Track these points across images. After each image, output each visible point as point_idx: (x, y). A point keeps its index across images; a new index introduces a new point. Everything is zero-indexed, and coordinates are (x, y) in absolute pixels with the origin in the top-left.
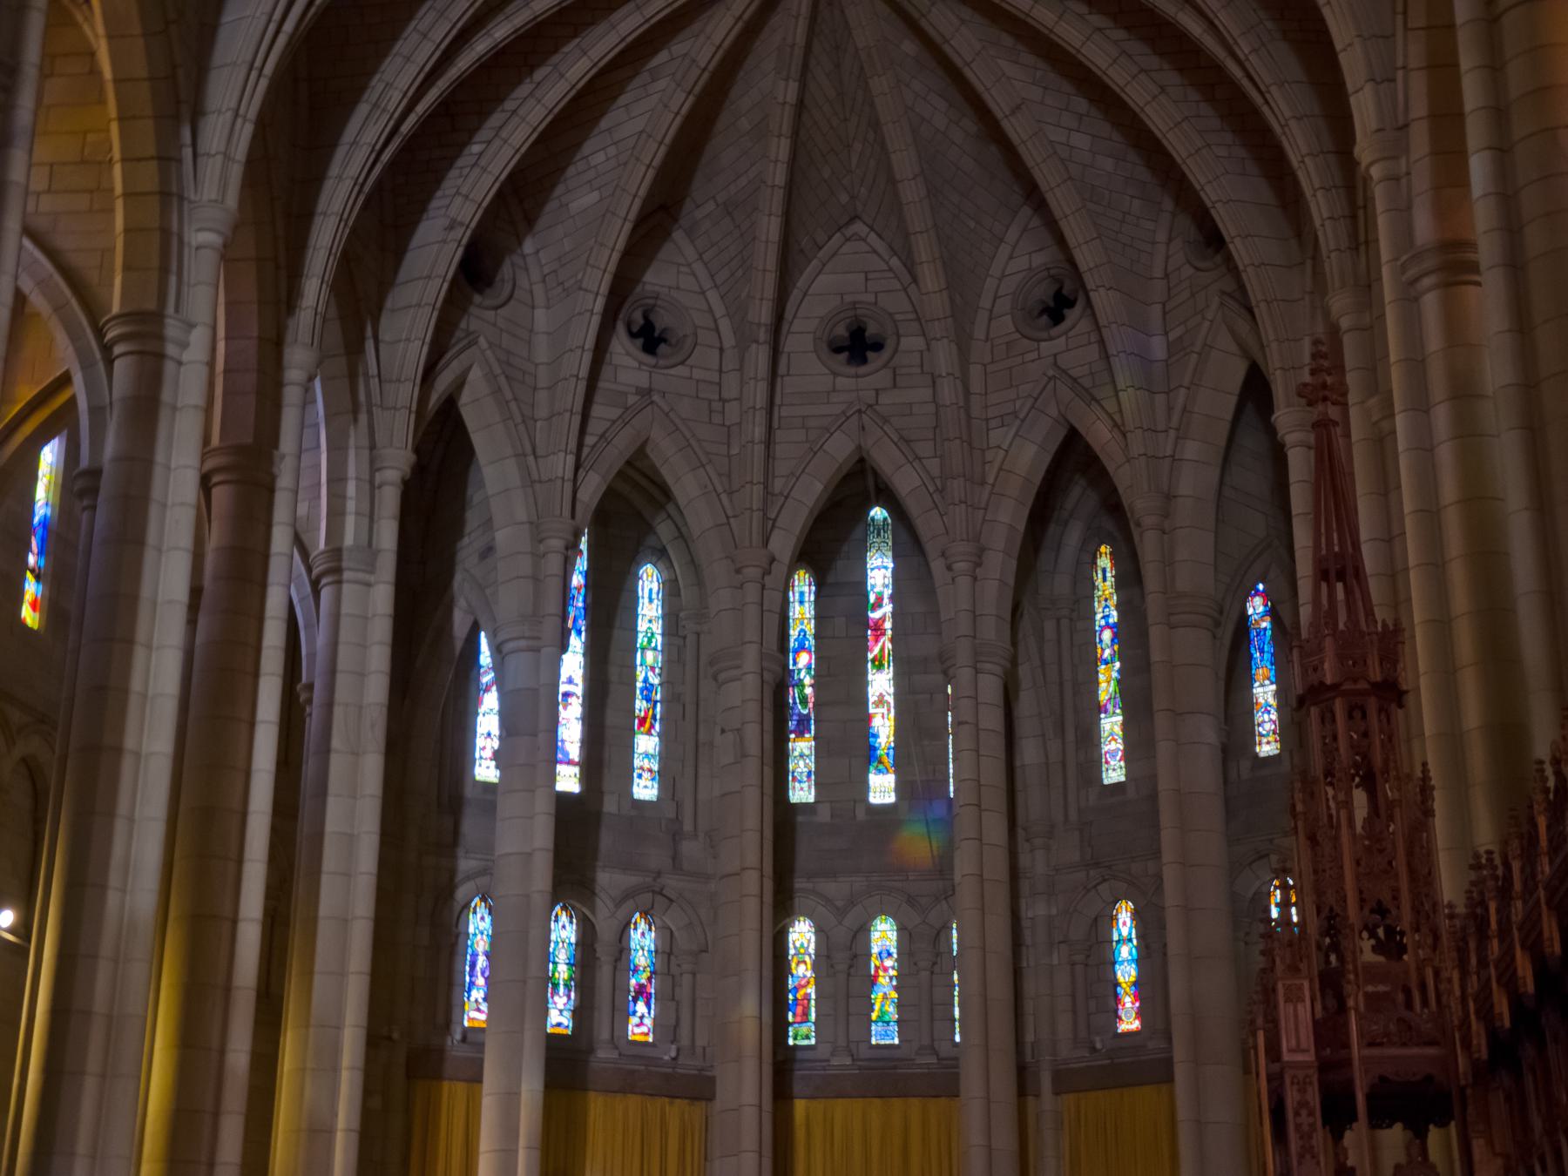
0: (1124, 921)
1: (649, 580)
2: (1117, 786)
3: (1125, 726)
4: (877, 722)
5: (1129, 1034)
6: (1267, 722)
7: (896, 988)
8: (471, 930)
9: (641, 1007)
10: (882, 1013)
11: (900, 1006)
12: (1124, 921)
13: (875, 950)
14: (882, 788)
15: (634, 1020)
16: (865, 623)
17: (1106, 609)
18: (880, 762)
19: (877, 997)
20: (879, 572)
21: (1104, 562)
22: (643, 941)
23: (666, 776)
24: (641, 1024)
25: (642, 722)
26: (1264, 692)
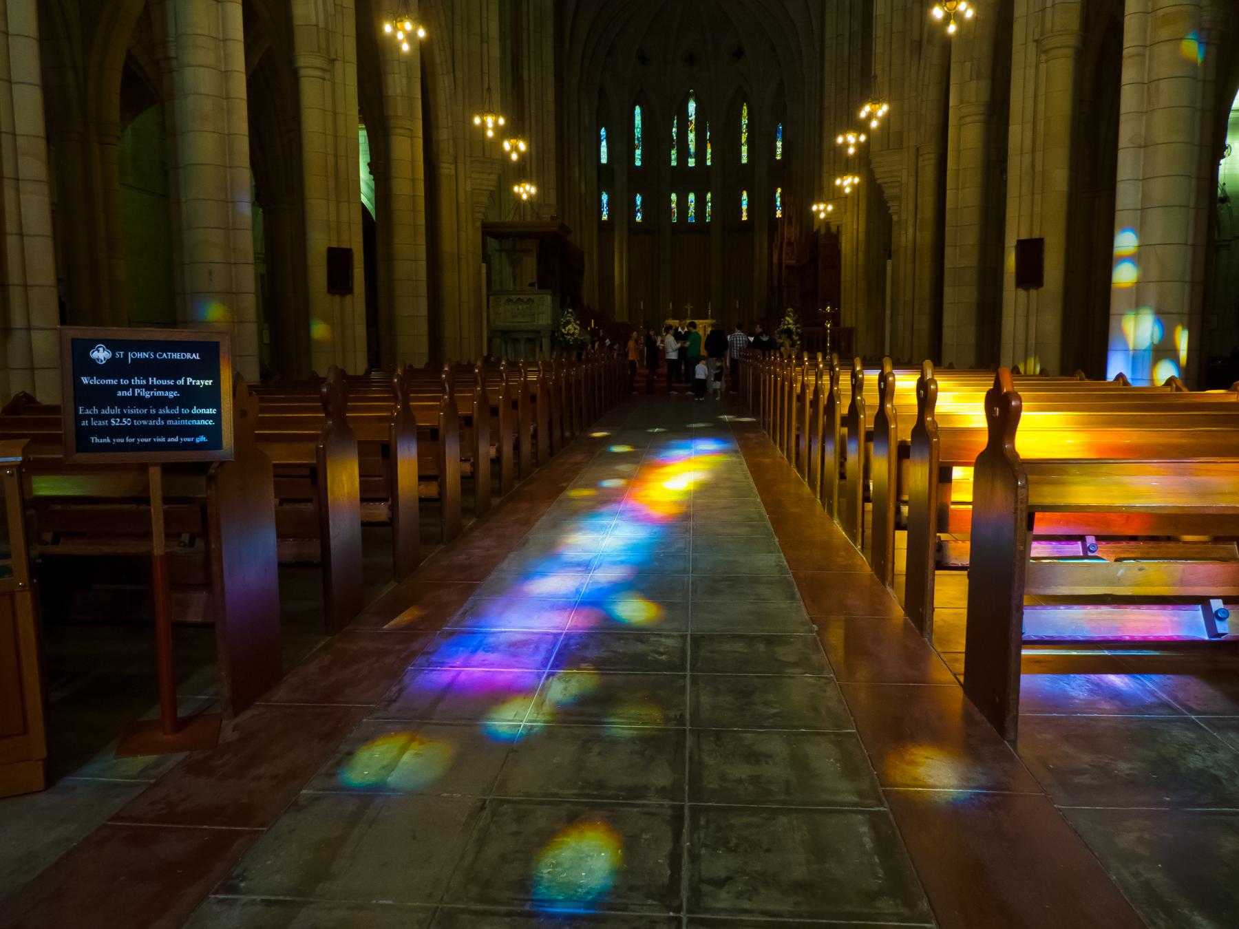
0: (745, 195)
1: (638, 110)
2: (744, 164)
6: (779, 151)
11: (695, 213)
12: (745, 195)
13: (689, 201)
14: (692, 162)
16: (688, 120)
17: (745, 121)
18: (691, 155)
19: (690, 211)
20: (692, 107)
21: (745, 107)
22: (639, 199)
23: (642, 160)
24: (639, 218)
26: (779, 144)
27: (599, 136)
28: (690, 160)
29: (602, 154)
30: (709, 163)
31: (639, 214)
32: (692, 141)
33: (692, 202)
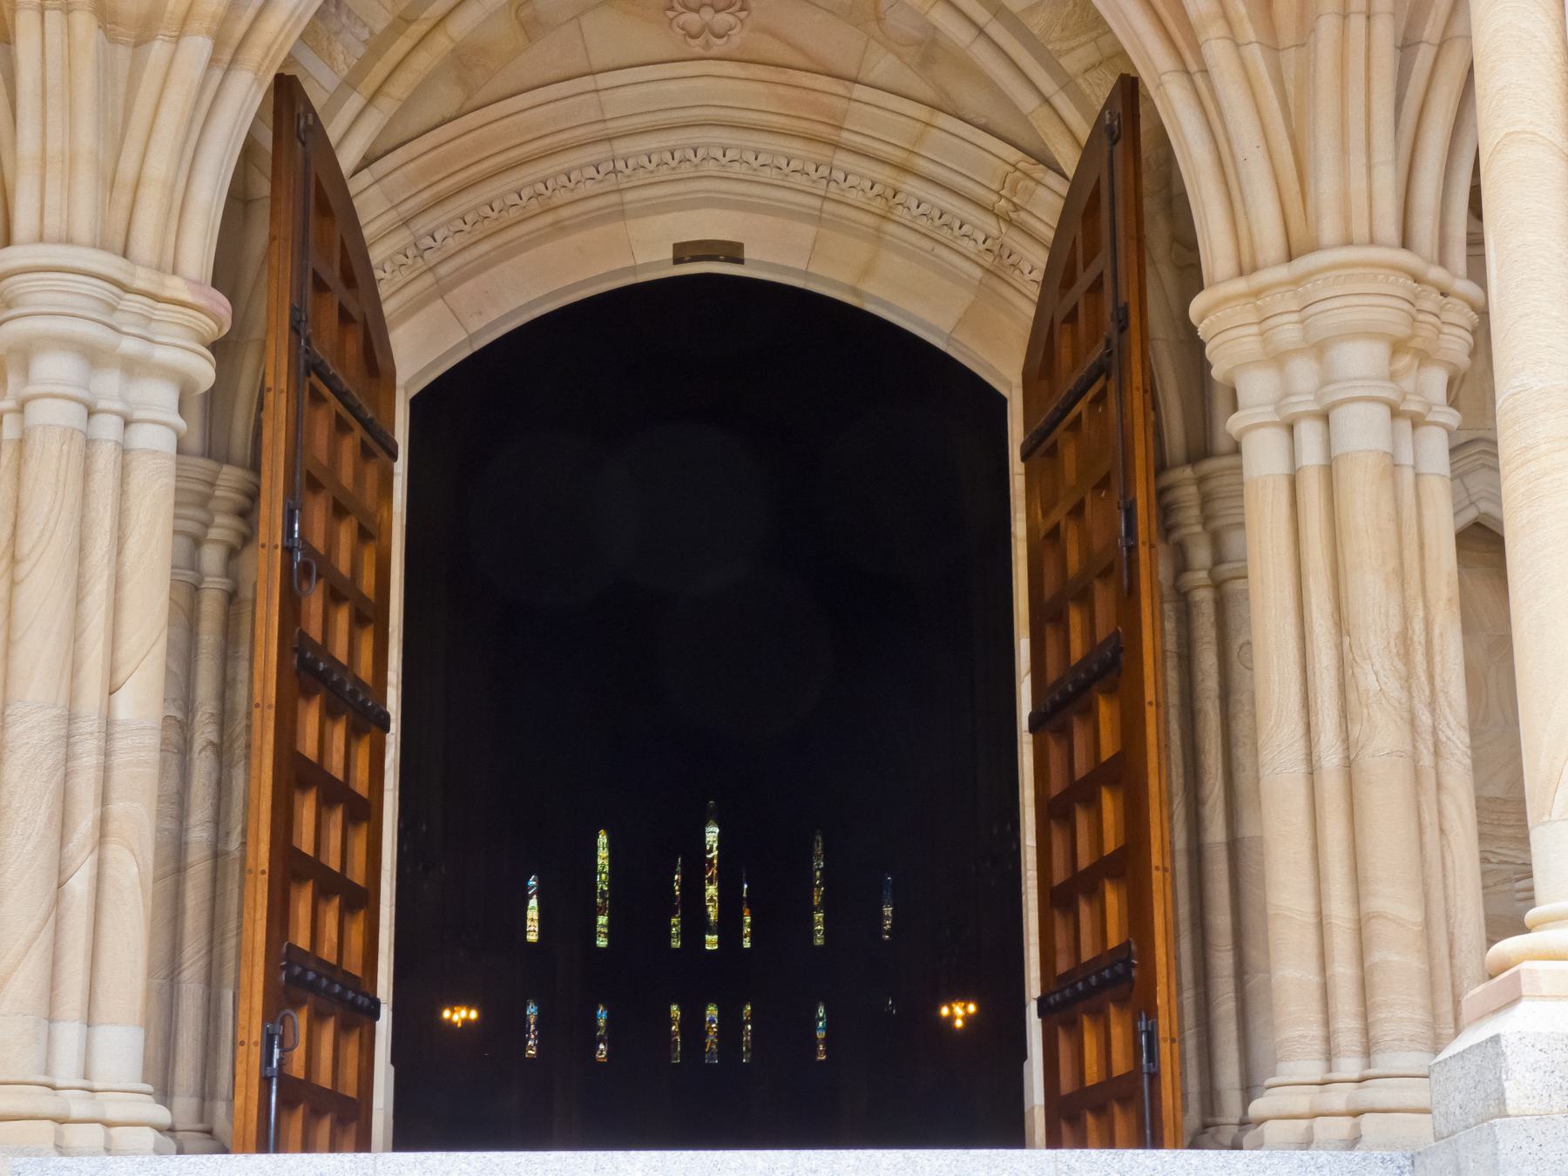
0: (821, 1012)
1: (603, 839)
3: (825, 918)
4: (710, 909)
5: (821, 1061)
7: (717, 1037)
8: (528, 1013)
9: (602, 1046)
10: (711, 1049)
11: (718, 1045)
12: (821, 1012)
14: (712, 942)
15: (599, 1052)
19: (708, 1041)
20: (712, 834)
22: (602, 1015)
25: (601, 908)
26: (888, 910)
27: (526, 888)
28: (708, 937)
29: (529, 923)
30: (747, 944)
31: (602, 1046)
32: (711, 900)
33: (712, 1021)
